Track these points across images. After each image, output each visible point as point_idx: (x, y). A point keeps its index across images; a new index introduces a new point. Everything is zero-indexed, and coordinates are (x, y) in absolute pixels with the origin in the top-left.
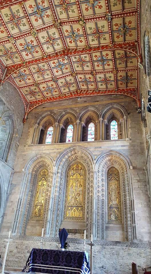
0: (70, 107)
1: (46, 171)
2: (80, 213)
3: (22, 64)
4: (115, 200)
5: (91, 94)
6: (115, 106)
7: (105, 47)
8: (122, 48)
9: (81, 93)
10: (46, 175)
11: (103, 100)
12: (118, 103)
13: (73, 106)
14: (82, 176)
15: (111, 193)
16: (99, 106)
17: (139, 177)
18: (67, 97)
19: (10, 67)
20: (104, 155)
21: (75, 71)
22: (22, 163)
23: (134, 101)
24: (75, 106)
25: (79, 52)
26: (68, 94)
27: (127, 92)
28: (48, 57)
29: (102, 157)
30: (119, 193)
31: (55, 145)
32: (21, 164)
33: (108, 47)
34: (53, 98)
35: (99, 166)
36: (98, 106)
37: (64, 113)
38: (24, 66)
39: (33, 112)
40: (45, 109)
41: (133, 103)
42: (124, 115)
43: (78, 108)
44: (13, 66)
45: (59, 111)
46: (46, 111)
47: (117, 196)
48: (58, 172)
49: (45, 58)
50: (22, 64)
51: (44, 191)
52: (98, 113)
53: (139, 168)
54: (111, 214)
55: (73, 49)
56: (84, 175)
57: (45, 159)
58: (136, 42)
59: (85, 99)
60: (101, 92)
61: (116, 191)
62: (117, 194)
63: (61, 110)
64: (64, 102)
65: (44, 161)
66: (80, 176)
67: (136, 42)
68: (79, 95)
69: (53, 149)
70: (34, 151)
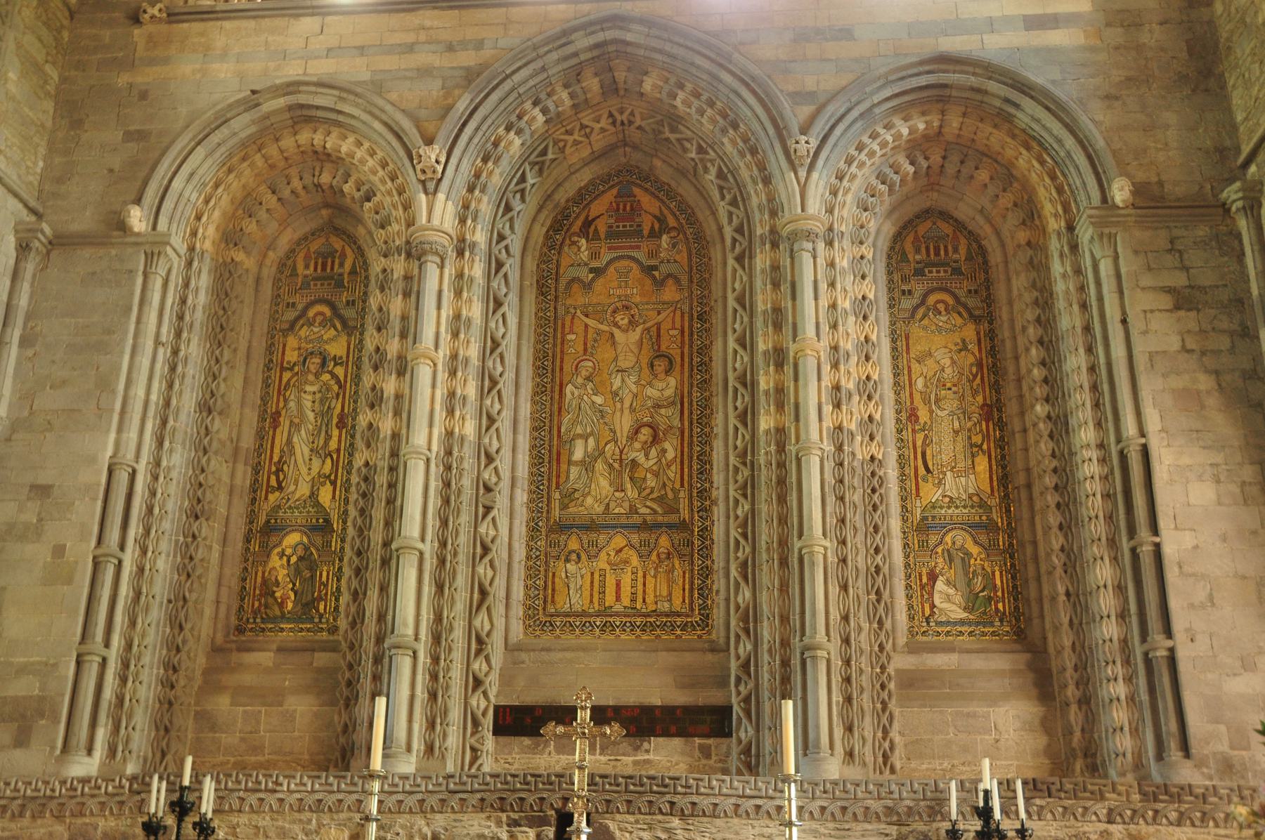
1: (337, 244)
4: (961, 465)
10: (340, 284)
14: (670, 281)
15: (923, 415)
17: (1186, 269)
20: (876, 99)
22: (116, 162)
29: (855, 113)
30: (993, 412)
32: (111, 171)
35: (834, 193)
47: (977, 439)
53: (1178, 200)
54: (933, 577)
56: (685, 282)
57: (335, 132)
61: (968, 392)
62: (975, 417)
65: (323, 157)
66: (648, 282)
69: (410, 48)
70: (224, 56)
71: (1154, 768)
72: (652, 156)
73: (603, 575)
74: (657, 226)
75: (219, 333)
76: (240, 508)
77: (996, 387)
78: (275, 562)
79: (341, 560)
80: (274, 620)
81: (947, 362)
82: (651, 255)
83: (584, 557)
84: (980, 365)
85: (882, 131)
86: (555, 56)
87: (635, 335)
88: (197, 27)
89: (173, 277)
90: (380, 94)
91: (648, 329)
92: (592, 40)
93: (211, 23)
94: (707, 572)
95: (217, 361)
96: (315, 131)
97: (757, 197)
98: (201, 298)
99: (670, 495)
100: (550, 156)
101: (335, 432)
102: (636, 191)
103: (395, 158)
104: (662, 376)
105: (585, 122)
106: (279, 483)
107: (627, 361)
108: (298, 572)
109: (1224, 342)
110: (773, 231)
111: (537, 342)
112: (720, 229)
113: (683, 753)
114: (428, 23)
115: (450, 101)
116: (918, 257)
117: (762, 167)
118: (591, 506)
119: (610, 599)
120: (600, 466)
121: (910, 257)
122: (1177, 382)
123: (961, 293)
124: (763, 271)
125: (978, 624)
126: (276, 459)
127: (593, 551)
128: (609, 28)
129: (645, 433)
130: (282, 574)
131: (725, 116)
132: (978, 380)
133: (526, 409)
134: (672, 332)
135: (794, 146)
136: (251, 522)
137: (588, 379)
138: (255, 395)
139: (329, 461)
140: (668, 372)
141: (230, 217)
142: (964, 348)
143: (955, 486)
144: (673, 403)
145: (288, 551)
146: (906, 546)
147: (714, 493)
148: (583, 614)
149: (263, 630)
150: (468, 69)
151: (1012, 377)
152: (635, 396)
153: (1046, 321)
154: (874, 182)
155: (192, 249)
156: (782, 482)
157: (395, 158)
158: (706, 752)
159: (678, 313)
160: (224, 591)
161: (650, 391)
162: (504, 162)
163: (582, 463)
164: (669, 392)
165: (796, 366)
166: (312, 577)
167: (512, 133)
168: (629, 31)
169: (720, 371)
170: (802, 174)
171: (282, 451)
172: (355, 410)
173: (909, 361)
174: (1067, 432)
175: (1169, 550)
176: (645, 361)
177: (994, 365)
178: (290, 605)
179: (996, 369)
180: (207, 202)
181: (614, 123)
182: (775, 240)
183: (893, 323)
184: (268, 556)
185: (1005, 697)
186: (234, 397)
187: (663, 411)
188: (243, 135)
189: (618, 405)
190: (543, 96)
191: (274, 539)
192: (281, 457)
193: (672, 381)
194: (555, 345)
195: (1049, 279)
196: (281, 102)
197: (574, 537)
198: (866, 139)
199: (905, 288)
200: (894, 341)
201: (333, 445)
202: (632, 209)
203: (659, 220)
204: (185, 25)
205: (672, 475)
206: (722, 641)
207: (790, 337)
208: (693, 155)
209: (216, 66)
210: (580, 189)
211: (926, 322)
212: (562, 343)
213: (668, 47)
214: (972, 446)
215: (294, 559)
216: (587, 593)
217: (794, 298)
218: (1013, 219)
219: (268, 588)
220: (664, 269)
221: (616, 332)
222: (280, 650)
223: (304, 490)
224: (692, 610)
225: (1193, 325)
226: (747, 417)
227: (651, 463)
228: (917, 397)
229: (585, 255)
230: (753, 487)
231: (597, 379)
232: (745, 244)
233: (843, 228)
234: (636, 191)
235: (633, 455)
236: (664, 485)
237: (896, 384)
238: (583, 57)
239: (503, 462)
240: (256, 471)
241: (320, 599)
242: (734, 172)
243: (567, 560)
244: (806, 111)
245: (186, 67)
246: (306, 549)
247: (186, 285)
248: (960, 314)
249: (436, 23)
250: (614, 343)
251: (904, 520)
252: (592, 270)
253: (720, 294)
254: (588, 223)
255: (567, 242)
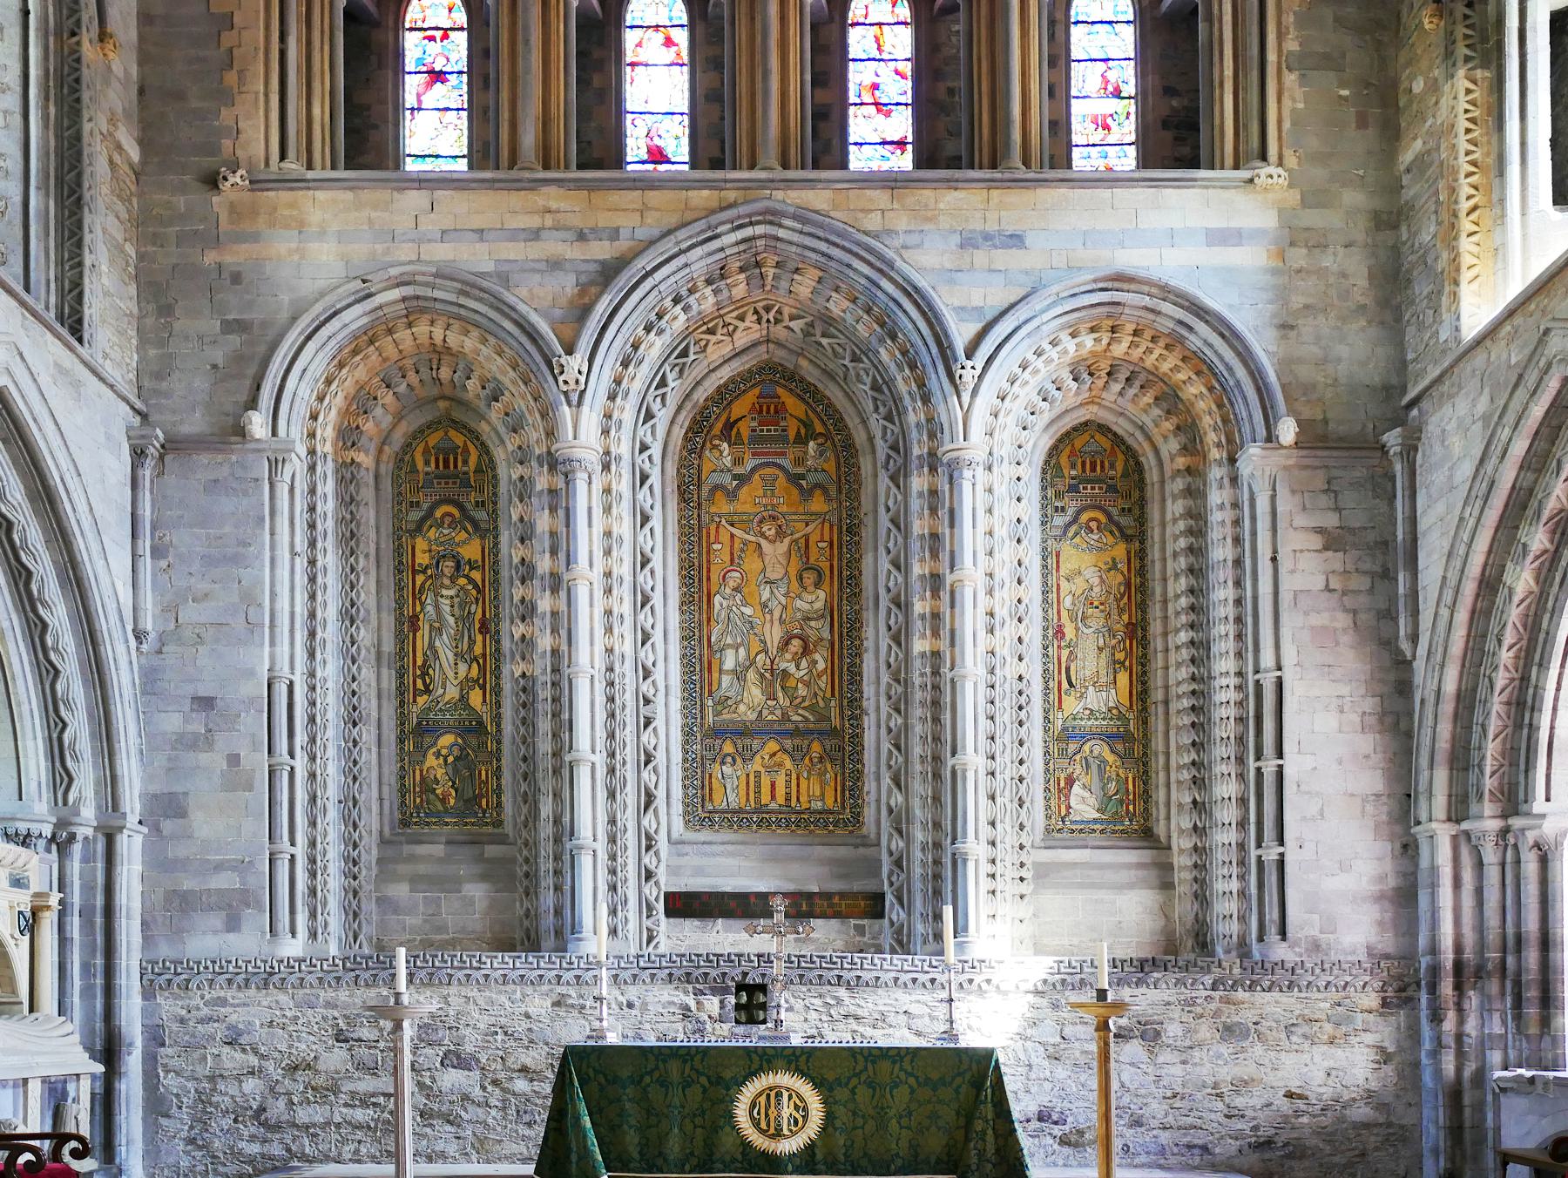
2: (823, 785)
4: (1103, 680)
14: (818, 492)
17: (1338, 509)
31: (552, 190)
47: (1120, 656)
48: (607, 453)
51: (479, 615)
54: (1070, 782)
61: (1115, 612)
65: (440, 353)
66: (795, 492)
69: (535, 235)
70: (322, 234)
71: (1255, 947)
72: (799, 355)
73: (758, 775)
74: (803, 431)
75: (349, 540)
76: (390, 710)
77: (1143, 607)
78: (431, 761)
79: (499, 760)
80: (438, 814)
81: (1096, 581)
82: (799, 462)
83: (739, 760)
84: (1128, 585)
85: (1048, 347)
86: (699, 251)
87: (783, 547)
88: (285, 196)
89: (297, 484)
90: (508, 288)
91: (796, 541)
92: (740, 234)
93: (301, 193)
94: (858, 776)
95: (353, 570)
96: (432, 323)
97: (914, 416)
98: (328, 506)
99: (821, 704)
100: (692, 357)
101: (479, 638)
102: (780, 391)
103: (528, 360)
104: (811, 588)
105: (728, 319)
106: (426, 686)
107: (775, 573)
108: (456, 771)
109: (1362, 583)
110: (932, 454)
111: (682, 551)
112: (871, 439)
113: (839, 932)
114: (554, 205)
115: (586, 300)
116: (1073, 473)
117: (921, 385)
118: (746, 713)
119: (765, 798)
120: (751, 675)
121: (1066, 472)
122: (1317, 620)
123: (1114, 511)
124: (921, 494)
125: (1109, 822)
126: (419, 662)
127: (748, 754)
128: (758, 223)
129: (796, 644)
130: (440, 773)
131: (882, 325)
132: (1126, 599)
133: (674, 618)
134: (824, 545)
135: (960, 371)
136: (402, 724)
137: (737, 589)
138: (389, 599)
139: (475, 665)
140: (817, 585)
141: (345, 413)
142: (1114, 567)
143: (1096, 700)
144: (823, 616)
145: (444, 752)
146: (1046, 753)
147: (865, 704)
148: (740, 811)
149: (428, 824)
150: (603, 263)
151: (1158, 597)
152: (785, 607)
153: (1197, 551)
154: (1037, 399)
155: (312, 452)
156: (936, 704)
157: (528, 360)
158: (860, 930)
159: (827, 525)
160: (386, 789)
161: (799, 603)
162: (645, 368)
163: (734, 672)
164: (819, 605)
165: (952, 593)
166: (472, 776)
167: (653, 334)
168: (780, 226)
169: (871, 588)
170: (966, 398)
171: (425, 654)
172: (497, 615)
173: (1058, 579)
174: (1208, 657)
175: (1288, 772)
176: (793, 572)
177: (1142, 584)
178: (452, 801)
179: (1143, 589)
180: (321, 399)
181: (759, 321)
182: (932, 462)
183: (1044, 541)
184: (424, 756)
185: (1131, 886)
186: (372, 603)
187: (813, 624)
188: (354, 327)
189: (768, 617)
190: (684, 292)
191: (428, 740)
192: (425, 661)
193: (822, 595)
194: (700, 554)
195: (1205, 507)
196: (395, 294)
197: (728, 742)
198: (1031, 357)
199: (1059, 504)
200: (1044, 559)
201: (478, 650)
202: (776, 412)
203: (805, 425)
204: (271, 194)
205: (823, 686)
206: (873, 836)
207: (947, 564)
208: (846, 362)
209: (314, 246)
210: (719, 387)
211: (1077, 540)
212: (708, 552)
213: (823, 246)
214: (1115, 662)
215: (450, 759)
216: (743, 793)
217: (952, 526)
218: (1173, 445)
219: (427, 786)
220: (812, 478)
221: (763, 542)
222: (448, 843)
223: (453, 692)
224: (844, 808)
225: (1338, 566)
226: (900, 638)
227: (802, 673)
228: (1064, 614)
229: (728, 461)
230: (906, 703)
231: (745, 590)
232: (900, 461)
233: (1004, 452)
234: (780, 391)
235: (783, 665)
236: (816, 694)
237: (1045, 601)
238: (728, 252)
239: (658, 674)
240: (401, 675)
241: (481, 796)
242: (890, 383)
243: (723, 763)
244: (972, 329)
245: (281, 245)
246: (462, 749)
247: (312, 491)
248: (1111, 532)
249: (563, 206)
250: (761, 555)
251: (1046, 731)
252: (735, 477)
253: (871, 507)
254: (730, 426)
255: (708, 445)
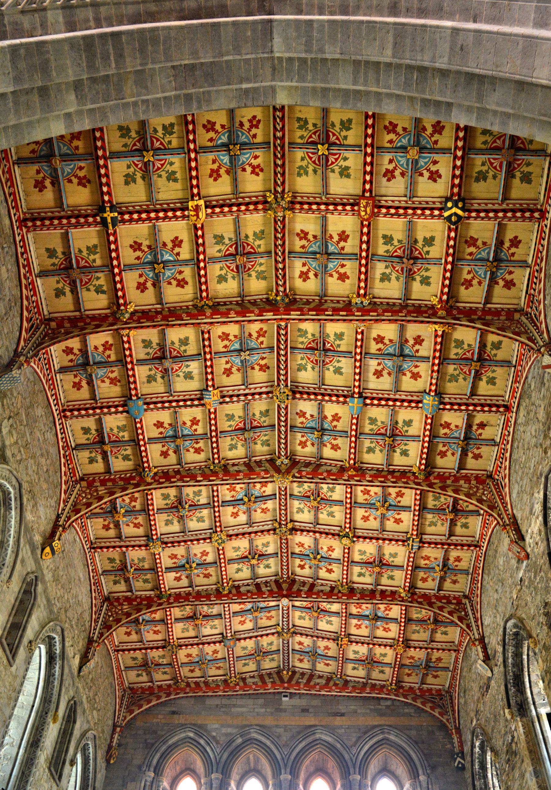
0: (261, 723)
3: (155, 599)
5: (322, 688)
6: (392, 737)
7: (389, 596)
8: (431, 604)
9: (293, 682)
11: (355, 712)
12: (401, 729)
13: (269, 721)
16: (347, 731)
18: (250, 687)
19: (118, 599)
21: (291, 626)
23: (443, 727)
24: (274, 723)
25: (321, 594)
26: (253, 677)
27: (421, 696)
28: (234, 591)
33: (397, 596)
34: (206, 683)
36: (343, 731)
37: (240, 740)
38: (160, 604)
39: (139, 723)
40: (178, 720)
41: (439, 735)
42: (420, 772)
43: (285, 731)
44: (127, 599)
45: (224, 731)
46: (183, 726)
49: (226, 592)
50: (155, 599)
52: (347, 756)
55: (304, 583)
58: (466, 597)
59: (303, 702)
60: (353, 687)
63: (229, 730)
64: (239, 702)
67: (466, 597)
68: (286, 685)
